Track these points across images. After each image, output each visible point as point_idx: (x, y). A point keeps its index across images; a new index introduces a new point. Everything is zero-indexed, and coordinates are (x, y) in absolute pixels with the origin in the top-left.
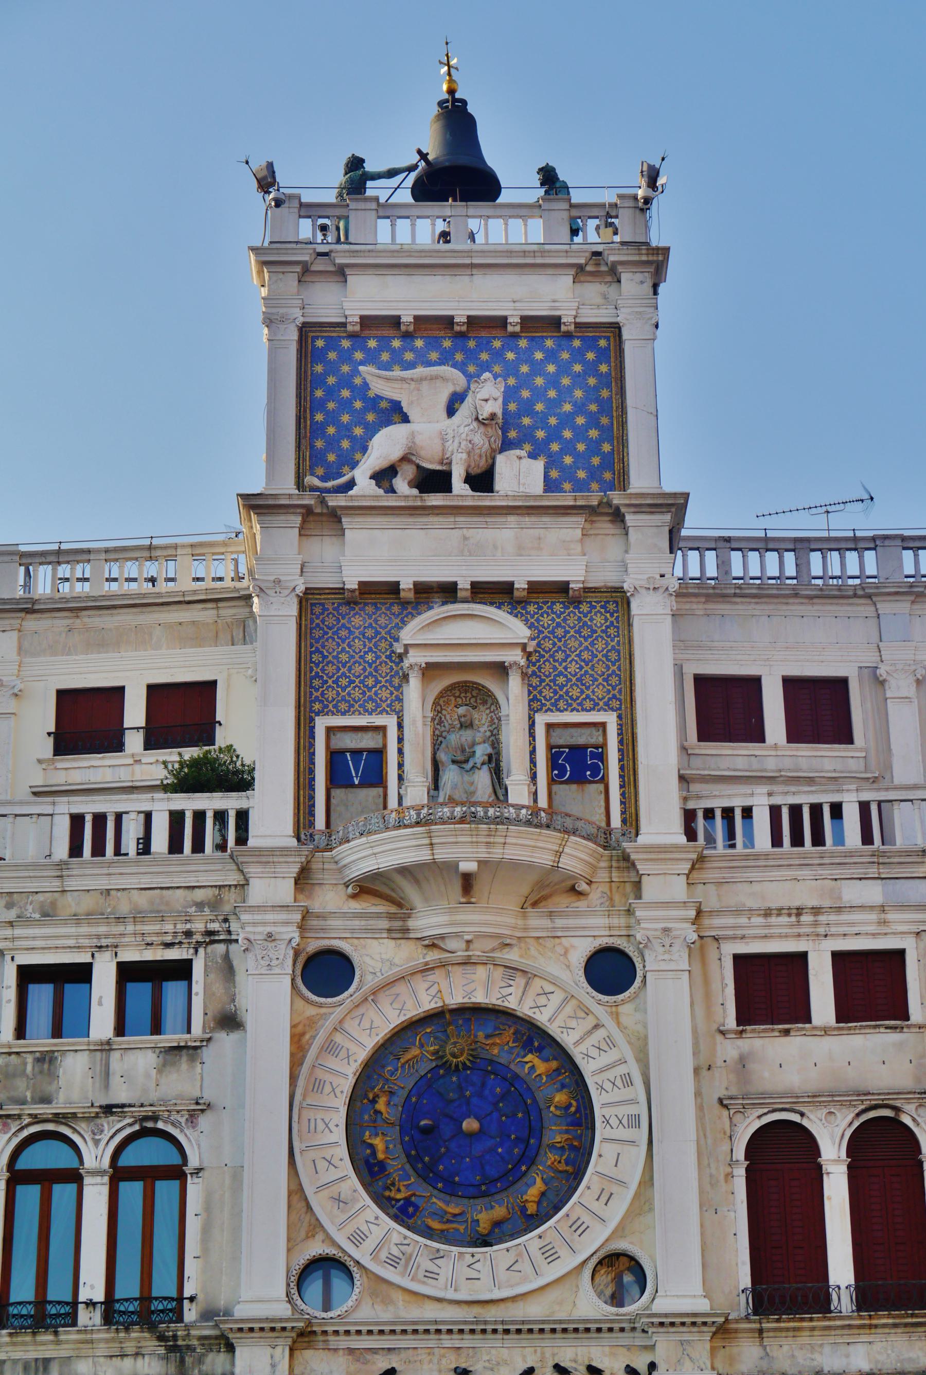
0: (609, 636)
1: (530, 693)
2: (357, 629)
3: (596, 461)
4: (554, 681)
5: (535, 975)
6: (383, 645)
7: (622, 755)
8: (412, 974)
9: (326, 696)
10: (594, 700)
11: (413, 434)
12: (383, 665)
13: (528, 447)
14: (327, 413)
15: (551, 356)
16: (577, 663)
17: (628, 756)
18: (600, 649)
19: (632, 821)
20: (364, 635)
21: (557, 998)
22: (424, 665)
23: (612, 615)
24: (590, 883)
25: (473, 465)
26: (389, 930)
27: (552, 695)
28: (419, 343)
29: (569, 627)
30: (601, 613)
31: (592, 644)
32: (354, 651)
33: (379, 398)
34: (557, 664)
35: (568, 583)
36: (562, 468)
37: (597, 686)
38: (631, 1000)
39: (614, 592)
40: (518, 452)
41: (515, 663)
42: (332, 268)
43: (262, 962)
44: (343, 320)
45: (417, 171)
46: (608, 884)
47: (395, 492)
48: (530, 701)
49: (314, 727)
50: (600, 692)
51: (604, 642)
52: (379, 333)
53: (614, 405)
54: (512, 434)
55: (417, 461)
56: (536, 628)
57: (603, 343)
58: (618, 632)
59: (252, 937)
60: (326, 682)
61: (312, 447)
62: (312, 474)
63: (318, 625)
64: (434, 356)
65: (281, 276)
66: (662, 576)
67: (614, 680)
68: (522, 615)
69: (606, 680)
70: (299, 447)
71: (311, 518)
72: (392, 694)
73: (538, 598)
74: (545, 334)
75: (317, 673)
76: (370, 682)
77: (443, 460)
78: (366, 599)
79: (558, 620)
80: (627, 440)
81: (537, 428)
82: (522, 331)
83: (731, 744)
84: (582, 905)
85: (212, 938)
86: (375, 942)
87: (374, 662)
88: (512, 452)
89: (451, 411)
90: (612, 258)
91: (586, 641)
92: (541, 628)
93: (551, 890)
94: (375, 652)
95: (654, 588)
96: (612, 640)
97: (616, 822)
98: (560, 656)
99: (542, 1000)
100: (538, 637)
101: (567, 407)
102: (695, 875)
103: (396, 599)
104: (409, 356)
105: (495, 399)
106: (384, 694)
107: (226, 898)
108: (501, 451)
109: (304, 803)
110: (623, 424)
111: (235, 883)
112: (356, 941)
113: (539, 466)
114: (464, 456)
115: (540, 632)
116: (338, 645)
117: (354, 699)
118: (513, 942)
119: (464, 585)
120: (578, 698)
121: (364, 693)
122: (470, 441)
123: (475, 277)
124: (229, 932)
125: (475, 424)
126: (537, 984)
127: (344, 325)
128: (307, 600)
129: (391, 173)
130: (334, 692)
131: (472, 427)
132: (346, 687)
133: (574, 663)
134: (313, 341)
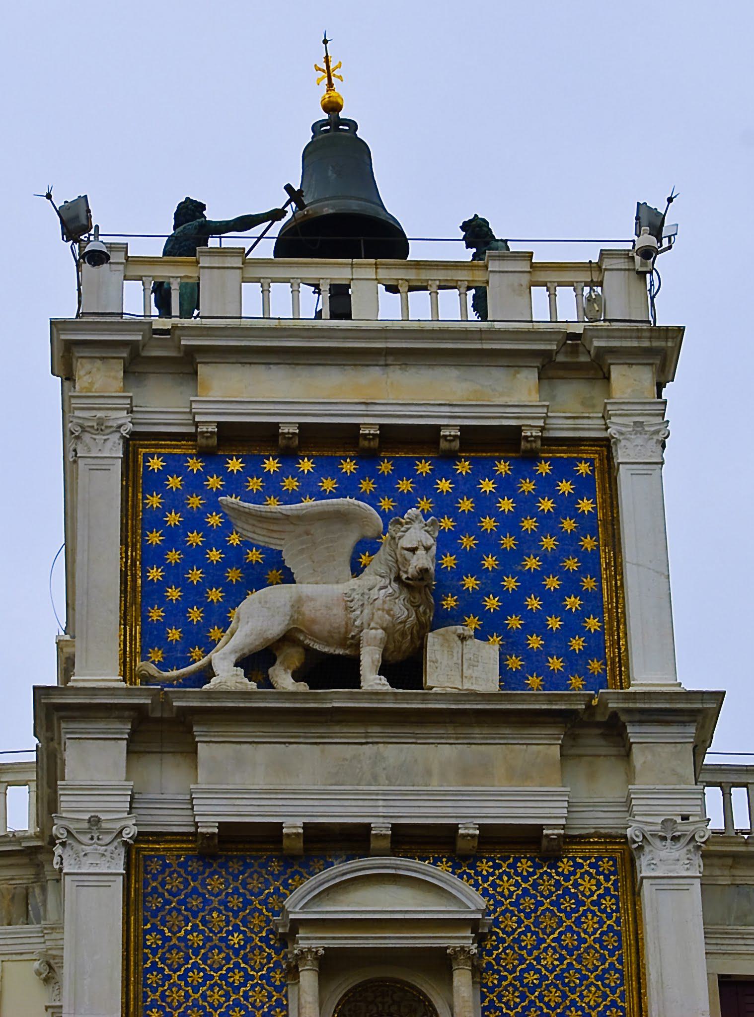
0: (604, 911)
1: (483, 997)
2: (217, 896)
3: (577, 644)
4: (520, 978)
11: (298, 604)
12: (257, 952)
13: (473, 623)
14: (168, 568)
15: (506, 487)
18: (590, 930)
22: (321, 952)
23: (607, 879)
25: (391, 647)
27: (518, 1000)
28: (306, 465)
30: (590, 874)
32: (211, 931)
33: (247, 544)
35: (541, 827)
36: (527, 655)
37: (588, 987)
39: (610, 843)
40: (460, 629)
44: (192, 430)
45: (284, 220)
47: (271, 686)
48: (484, 1009)
50: (591, 999)
51: (596, 919)
53: (603, 560)
54: (450, 602)
55: (307, 641)
56: (492, 897)
57: (583, 468)
58: (617, 904)
60: (169, 977)
61: (145, 618)
62: (145, 658)
63: (155, 889)
64: (328, 485)
65: (99, 363)
66: (685, 818)
67: (613, 979)
68: (470, 877)
72: (270, 996)
73: (493, 851)
75: (154, 964)
76: (237, 978)
77: (346, 639)
78: (228, 850)
80: (624, 612)
82: (462, 450)
87: (243, 947)
88: (453, 628)
89: (357, 569)
90: (597, 343)
91: (569, 917)
94: (244, 932)
95: (675, 839)
96: (609, 917)
98: (529, 940)
100: (495, 911)
101: (532, 563)
103: (275, 850)
104: (291, 484)
105: (427, 549)
108: (433, 627)
110: (619, 590)
113: (491, 650)
115: (498, 903)
117: (211, 1005)
119: (381, 826)
120: (558, 1006)
121: (227, 995)
125: (395, 585)
127: (191, 437)
129: (245, 223)
134: (146, 461)
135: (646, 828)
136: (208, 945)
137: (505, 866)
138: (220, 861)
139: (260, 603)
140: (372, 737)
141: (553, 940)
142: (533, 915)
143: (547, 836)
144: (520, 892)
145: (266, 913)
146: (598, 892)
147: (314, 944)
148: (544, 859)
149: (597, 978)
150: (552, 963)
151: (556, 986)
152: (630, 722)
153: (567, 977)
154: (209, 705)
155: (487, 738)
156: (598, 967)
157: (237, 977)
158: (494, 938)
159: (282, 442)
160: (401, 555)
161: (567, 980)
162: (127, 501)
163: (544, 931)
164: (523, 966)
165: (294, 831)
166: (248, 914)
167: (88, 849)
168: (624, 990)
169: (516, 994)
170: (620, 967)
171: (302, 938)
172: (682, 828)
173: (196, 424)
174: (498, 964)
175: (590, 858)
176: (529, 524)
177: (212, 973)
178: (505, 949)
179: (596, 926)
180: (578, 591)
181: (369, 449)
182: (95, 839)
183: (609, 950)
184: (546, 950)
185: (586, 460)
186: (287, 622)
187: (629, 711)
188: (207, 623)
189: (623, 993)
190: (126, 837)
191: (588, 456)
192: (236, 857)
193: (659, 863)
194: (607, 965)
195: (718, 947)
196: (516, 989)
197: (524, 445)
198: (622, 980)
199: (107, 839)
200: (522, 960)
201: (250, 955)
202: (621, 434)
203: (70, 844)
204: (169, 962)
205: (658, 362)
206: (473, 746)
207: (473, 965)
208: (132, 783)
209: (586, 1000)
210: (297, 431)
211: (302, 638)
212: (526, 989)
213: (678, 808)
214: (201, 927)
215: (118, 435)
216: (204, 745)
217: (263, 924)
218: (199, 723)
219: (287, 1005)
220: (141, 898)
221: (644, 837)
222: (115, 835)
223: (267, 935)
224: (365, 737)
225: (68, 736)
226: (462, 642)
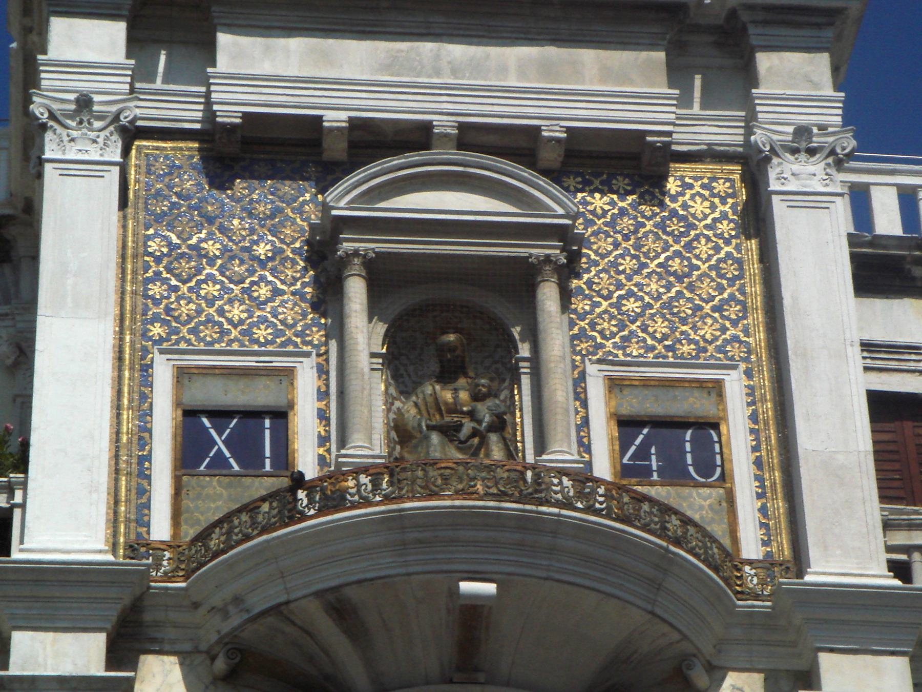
0: (720, 236)
1: (572, 324)
4: (618, 306)
7: (757, 439)
18: (704, 256)
27: (615, 329)
29: (643, 216)
31: (689, 247)
37: (703, 318)
41: (548, 259)
49: (151, 366)
50: (707, 331)
51: (710, 245)
66: (822, 128)
67: (733, 311)
75: (157, 274)
76: (264, 291)
79: (621, 204)
96: (728, 242)
98: (628, 264)
109: (128, 501)
116: (199, 227)
117: (230, 321)
120: (665, 337)
130: (193, 306)
135: (775, 137)
137: (597, 183)
138: (242, 164)
141: (660, 265)
144: (615, 211)
145: (301, 223)
150: (657, 291)
152: (751, 22)
153: (676, 307)
156: (714, 297)
161: (675, 310)
163: (646, 255)
164: (623, 292)
167: (75, 134)
168: (748, 324)
169: (613, 322)
170: (742, 298)
171: (348, 240)
174: (590, 288)
175: (701, 178)
178: (597, 274)
179: (711, 252)
182: (85, 124)
183: (728, 279)
187: (751, 7)
190: (124, 121)
194: (725, 295)
196: (612, 317)
199: (97, 124)
200: (620, 286)
201: (280, 268)
203: (52, 127)
221: (771, 146)
222: (108, 120)
223: (301, 247)
225: (52, 9)
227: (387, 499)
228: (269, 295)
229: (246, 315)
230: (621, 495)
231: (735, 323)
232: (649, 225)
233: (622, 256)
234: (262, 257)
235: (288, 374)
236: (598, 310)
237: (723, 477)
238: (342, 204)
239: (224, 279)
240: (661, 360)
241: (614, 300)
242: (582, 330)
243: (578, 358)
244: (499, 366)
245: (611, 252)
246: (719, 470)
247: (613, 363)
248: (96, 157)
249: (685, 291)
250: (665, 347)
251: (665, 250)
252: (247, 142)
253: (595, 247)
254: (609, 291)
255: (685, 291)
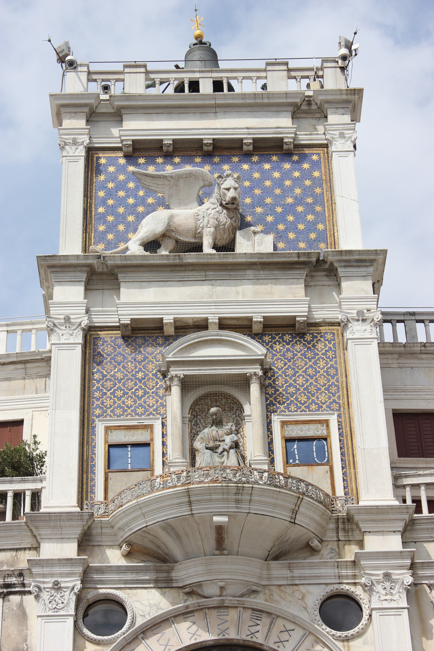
1: (267, 399)
5: (278, 616)
6: (150, 366)
8: (175, 617)
9: (105, 404)
10: (318, 404)
11: (171, 218)
12: (151, 381)
16: (304, 377)
17: (347, 445)
18: (321, 367)
19: (352, 492)
20: (135, 360)
21: (297, 634)
22: (182, 376)
24: (321, 541)
26: (156, 581)
32: (127, 371)
34: (288, 378)
35: (295, 317)
36: (288, 241)
37: (321, 394)
38: (359, 635)
39: (331, 326)
41: (255, 374)
42: (111, 111)
43: (50, 605)
44: (120, 145)
46: (336, 543)
48: (267, 405)
49: (95, 427)
50: (322, 398)
51: (324, 362)
52: (147, 154)
53: (325, 198)
57: (315, 157)
58: (335, 354)
59: (42, 586)
60: (106, 394)
65: (73, 115)
69: (327, 389)
70: (86, 230)
71: (94, 277)
72: (157, 401)
74: (271, 153)
76: (140, 393)
78: (137, 334)
80: (336, 221)
81: (267, 215)
83: (425, 459)
84: (315, 560)
85: (9, 590)
86: (145, 591)
87: (144, 379)
91: (310, 361)
92: (274, 353)
93: (288, 551)
97: (340, 492)
99: (285, 636)
101: (290, 200)
102: (407, 534)
103: (160, 333)
106: (151, 402)
107: (22, 558)
110: (333, 211)
111: (29, 546)
112: (128, 591)
113: (270, 239)
114: (212, 229)
117: (127, 406)
118: (259, 589)
119: (213, 319)
120: (305, 402)
121: (135, 401)
122: (217, 219)
123: (218, 114)
124: (24, 585)
125: (220, 208)
126: (280, 623)
128: (91, 335)
130: (112, 401)
131: (217, 209)
132: (121, 397)
133: (301, 377)
135: (349, 315)
136: (126, 378)
137: (277, 338)
138: (132, 339)
139: (152, 217)
140: (208, 277)
142: (292, 360)
143: (298, 321)
146: (325, 349)
147: (178, 373)
148: (298, 334)
149: (325, 389)
151: (305, 394)
154: (125, 262)
155: (267, 276)
156: (326, 384)
157: (140, 393)
158: (272, 371)
159: (165, 149)
160: (222, 192)
161: (310, 391)
162: (88, 178)
164: (288, 384)
165: (169, 321)
166: (147, 363)
167: (64, 332)
170: (337, 384)
172: (367, 315)
173: (122, 141)
176: (288, 183)
177: (128, 391)
179: (324, 365)
180: (313, 212)
181: (208, 151)
184: (299, 377)
185: (316, 154)
186: (166, 226)
188: (127, 231)
189: (339, 397)
191: (317, 152)
192: (140, 337)
193: (355, 332)
194: (330, 383)
195: (392, 396)
197: (285, 147)
198: (338, 390)
201: (147, 382)
202: (333, 138)
204: (105, 386)
205: (351, 107)
206: (260, 280)
207: (261, 383)
208: (86, 300)
209: (320, 399)
210: (172, 142)
211: (174, 235)
212: (289, 395)
213: (365, 306)
214: (122, 370)
215: (82, 146)
216: (124, 283)
217: (154, 368)
218: (121, 272)
219: (166, 405)
220: (92, 357)
221: (348, 319)
222: (77, 325)
224: (206, 277)
226: (254, 235)
227: (183, 485)
228: (143, 394)
229: (133, 403)
230: (279, 477)
231: (334, 395)
232: (299, 355)
233: (287, 369)
234: (140, 378)
235: (150, 427)
236: (278, 393)
237: (328, 460)
238: (170, 356)
239: (125, 388)
240: (303, 412)
241: (284, 388)
242: (271, 401)
243: (269, 413)
244: (238, 418)
245: (283, 367)
246: (326, 459)
247: (283, 415)
248: (73, 342)
249: (314, 382)
250: (305, 407)
251: (306, 365)
252: (134, 329)
253: (276, 366)
254: (282, 384)
255: (314, 382)
